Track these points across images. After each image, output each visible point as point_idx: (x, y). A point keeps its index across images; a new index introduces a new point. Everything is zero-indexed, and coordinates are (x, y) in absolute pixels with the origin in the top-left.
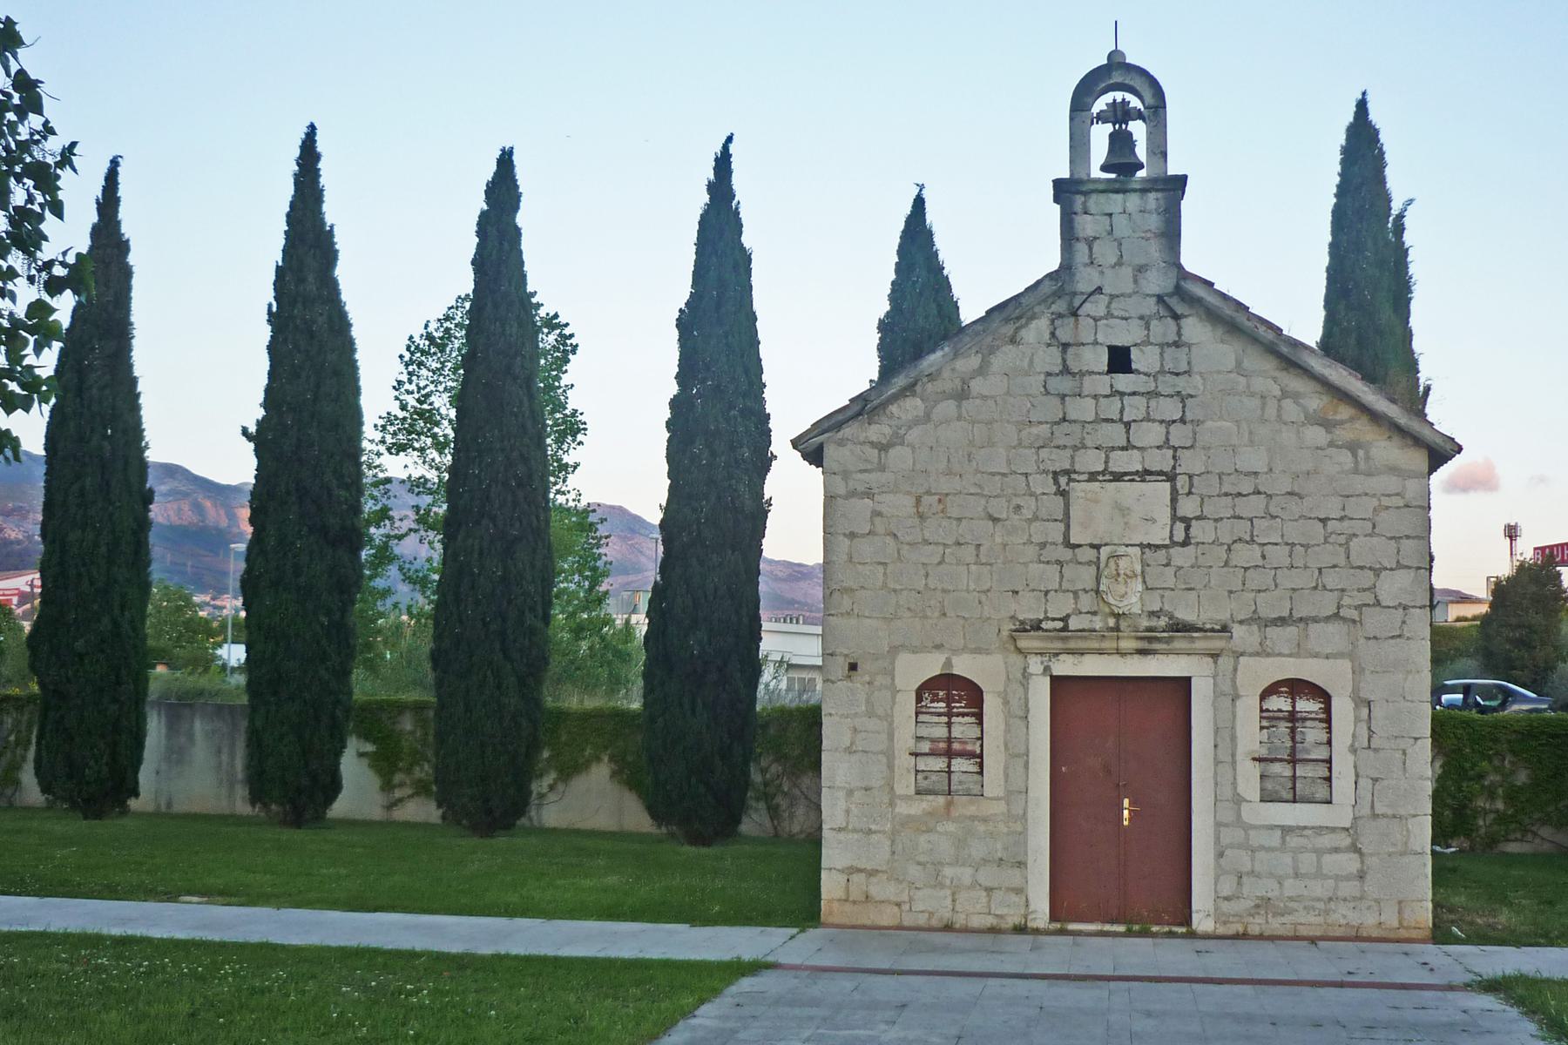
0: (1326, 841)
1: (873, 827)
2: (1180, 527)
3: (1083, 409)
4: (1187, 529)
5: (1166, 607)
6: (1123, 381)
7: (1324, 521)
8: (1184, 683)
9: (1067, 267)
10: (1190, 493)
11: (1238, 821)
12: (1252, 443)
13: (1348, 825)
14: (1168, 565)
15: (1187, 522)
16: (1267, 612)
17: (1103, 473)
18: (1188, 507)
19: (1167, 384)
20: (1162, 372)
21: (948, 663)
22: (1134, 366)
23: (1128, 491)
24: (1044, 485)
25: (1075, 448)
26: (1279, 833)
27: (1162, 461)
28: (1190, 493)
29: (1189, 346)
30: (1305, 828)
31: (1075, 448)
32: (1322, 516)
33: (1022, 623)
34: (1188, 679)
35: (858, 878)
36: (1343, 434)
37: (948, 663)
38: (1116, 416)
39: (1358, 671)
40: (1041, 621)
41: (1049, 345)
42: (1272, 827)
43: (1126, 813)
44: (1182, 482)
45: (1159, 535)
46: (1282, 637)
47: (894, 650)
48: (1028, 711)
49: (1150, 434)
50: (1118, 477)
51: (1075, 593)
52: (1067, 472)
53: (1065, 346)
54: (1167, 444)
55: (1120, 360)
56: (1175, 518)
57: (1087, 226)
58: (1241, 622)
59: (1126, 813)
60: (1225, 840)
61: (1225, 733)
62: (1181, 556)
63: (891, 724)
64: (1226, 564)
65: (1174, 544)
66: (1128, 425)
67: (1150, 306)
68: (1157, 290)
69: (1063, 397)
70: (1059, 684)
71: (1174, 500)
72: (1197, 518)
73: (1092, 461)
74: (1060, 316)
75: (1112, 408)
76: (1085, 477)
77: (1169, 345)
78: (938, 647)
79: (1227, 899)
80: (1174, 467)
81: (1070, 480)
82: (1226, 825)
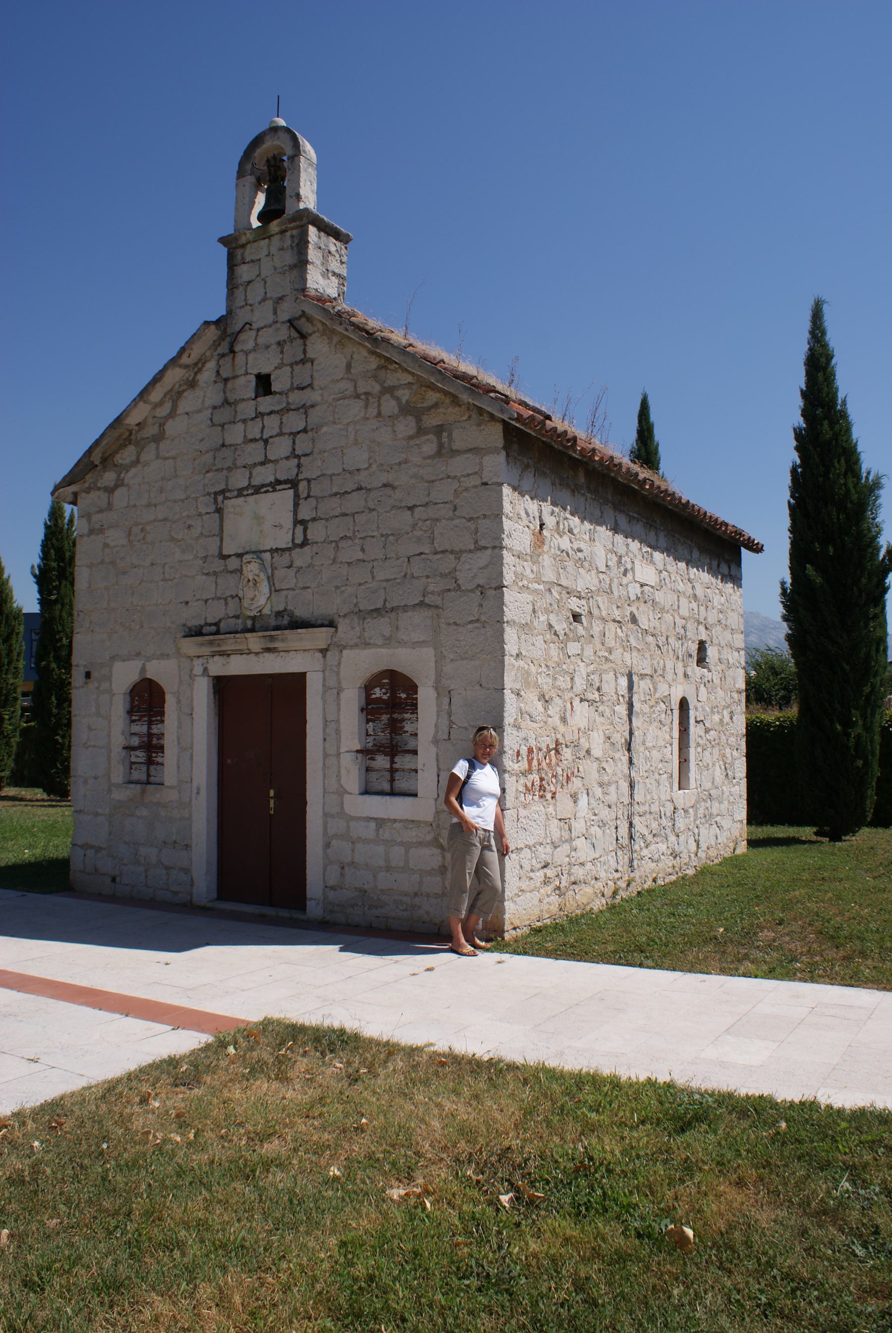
0: (411, 835)
1: (100, 810)
2: (300, 528)
3: (236, 434)
4: (305, 530)
5: (289, 607)
6: (266, 403)
7: (411, 509)
8: (299, 679)
9: (230, 312)
10: (309, 496)
11: (341, 814)
12: (356, 442)
13: (430, 818)
14: (289, 567)
15: (303, 523)
16: (365, 606)
17: (247, 488)
18: (305, 513)
19: (296, 398)
20: (292, 389)
21: (143, 670)
22: (274, 388)
23: (266, 500)
24: (205, 505)
25: (229, 469)
26: (373, 825)
27: (287, 469)
28: (309, 496)
29: (312, 361)
30: (395, 821)
31: (229, 469)
32: (410, 505)
33: (190, 629)
34: (303, 675)
35: (90, 853)
36: (431, 421)
37: (143, 670)
38: (258, 437)
39: (440, 659)
40: (202, 627)
41: (215, 382)
42: (369, 819)
43: (272, 802)
44: (303, 486)
45: (284, 540)
46: (381, 626)
47: (113, 658)
48: (192, 709)
49: (280, 448)
50: (257, 490)
51: (226, 599)
52: (223, 492)
53: (226, 380)
54: (294, 455)
55: (264, 384)
56: (297, 522)
57: (245, 272)
58: (345, 616)
59: (272, 802)
60: (331, 832)
61: (330, 724)
62: (301, 558)
63: (110, 721)
64: (334, 561)
65: (296, 546)
66: (266, 442)
67: (284, 333)
68: (287, 318)
69: (222, 426)
70: (223, 687)
71: (296, 505)
72: (314, 520)
73: (239, 480)
74: (223, 356)
75: (254, 430)
76: (236, 493)
77: (297, 363)
78: (138, 654)
79: (332, 888)
80: (297, 475)
81: (226, 498)
82: (332, 816)
